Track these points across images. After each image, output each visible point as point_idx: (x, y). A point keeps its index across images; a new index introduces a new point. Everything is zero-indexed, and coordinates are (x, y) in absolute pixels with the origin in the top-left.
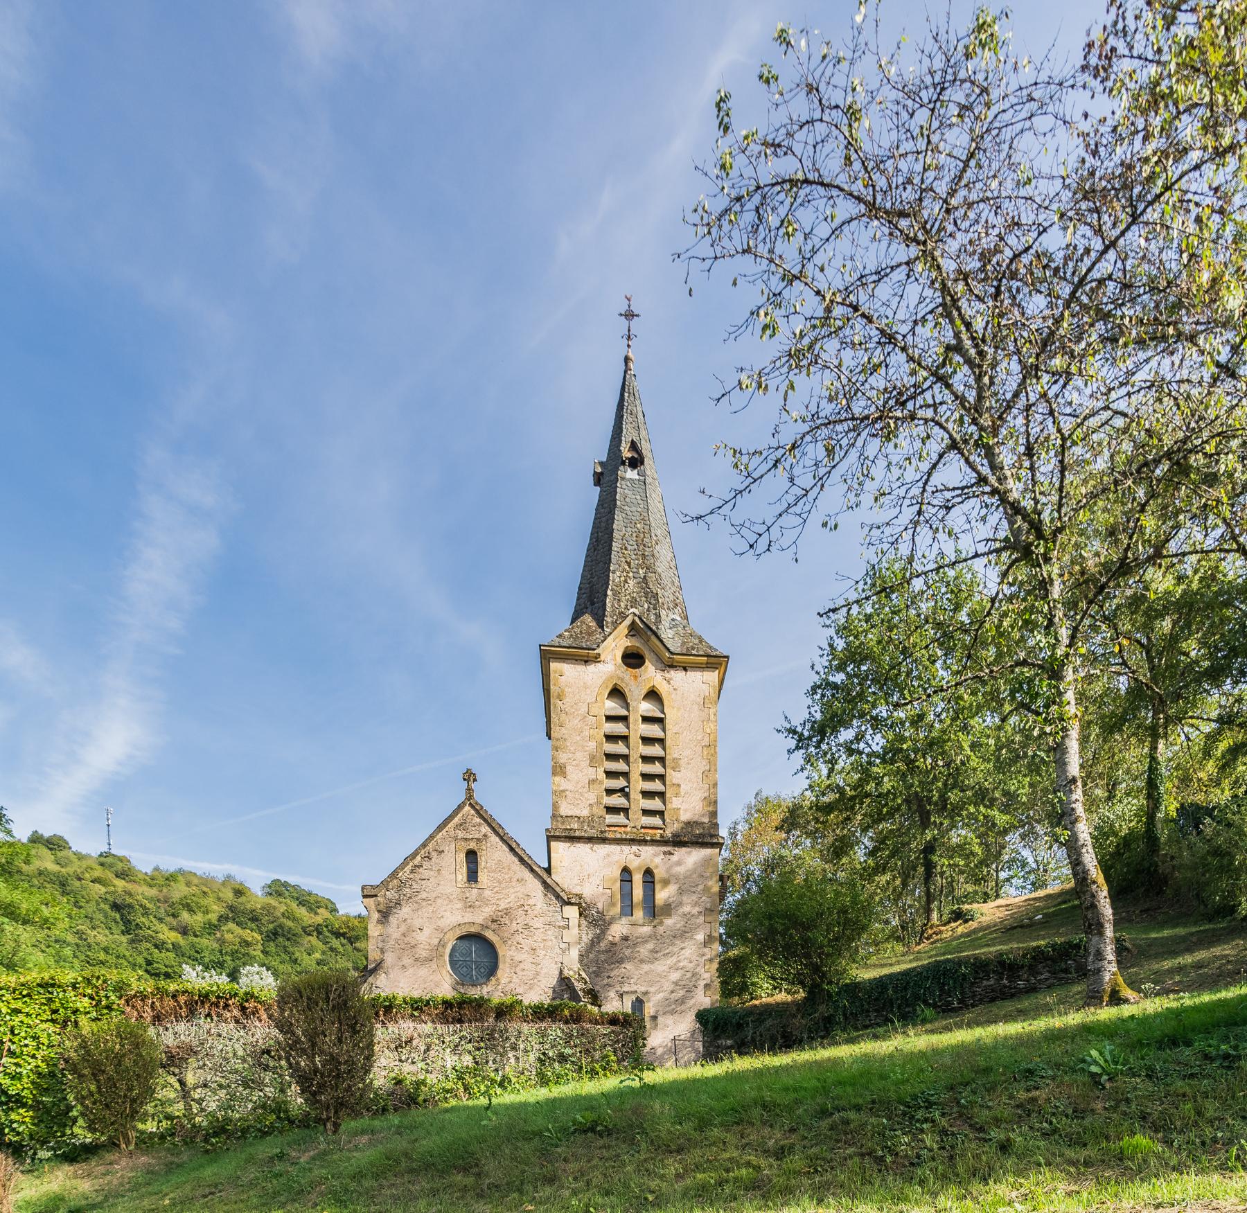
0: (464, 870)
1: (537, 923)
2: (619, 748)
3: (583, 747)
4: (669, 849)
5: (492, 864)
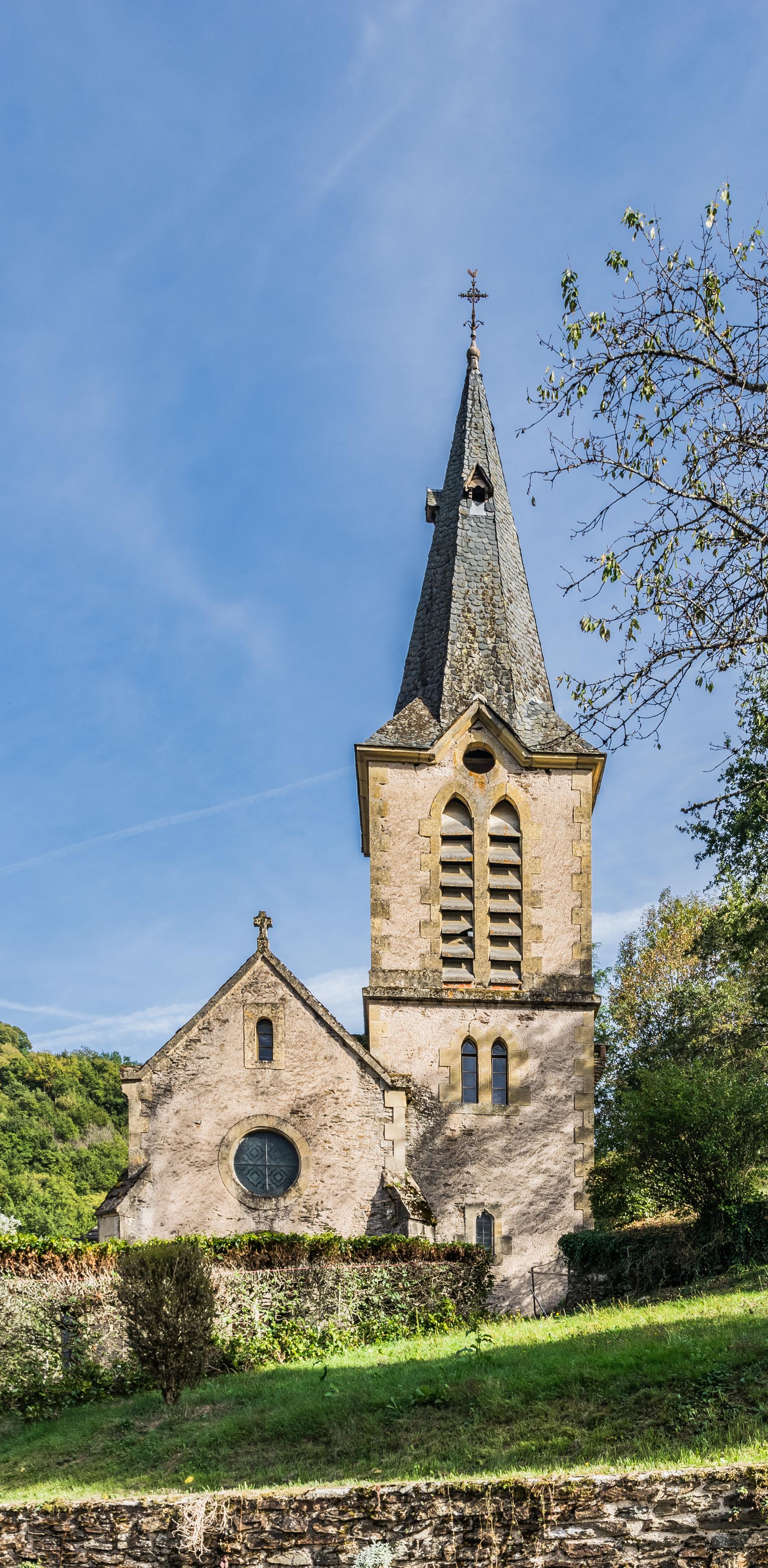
0: (255, 1045)
1: (351, 1115)
2: (460, 879)
3: (412, 878)
4: (527, 1012)
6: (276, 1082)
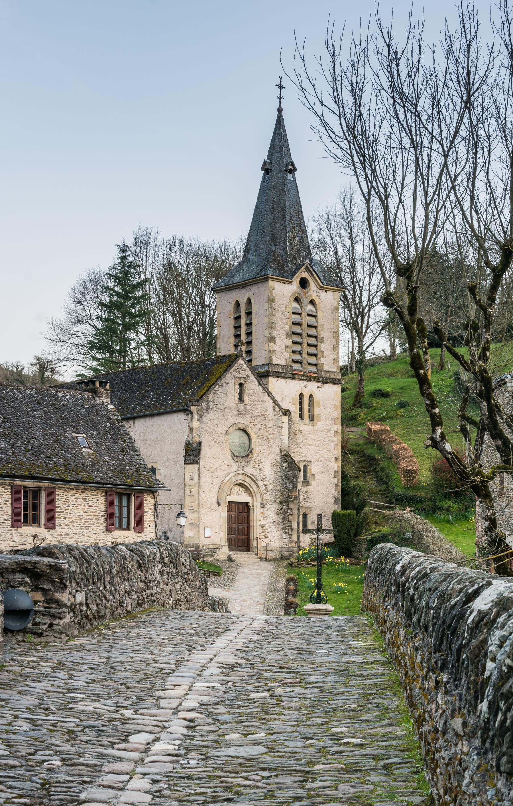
1: (270, 425)
2: (297, 329)
3: (283, 328)
4: (320, 384)
5: (250, 392)
6: (245, 409)
